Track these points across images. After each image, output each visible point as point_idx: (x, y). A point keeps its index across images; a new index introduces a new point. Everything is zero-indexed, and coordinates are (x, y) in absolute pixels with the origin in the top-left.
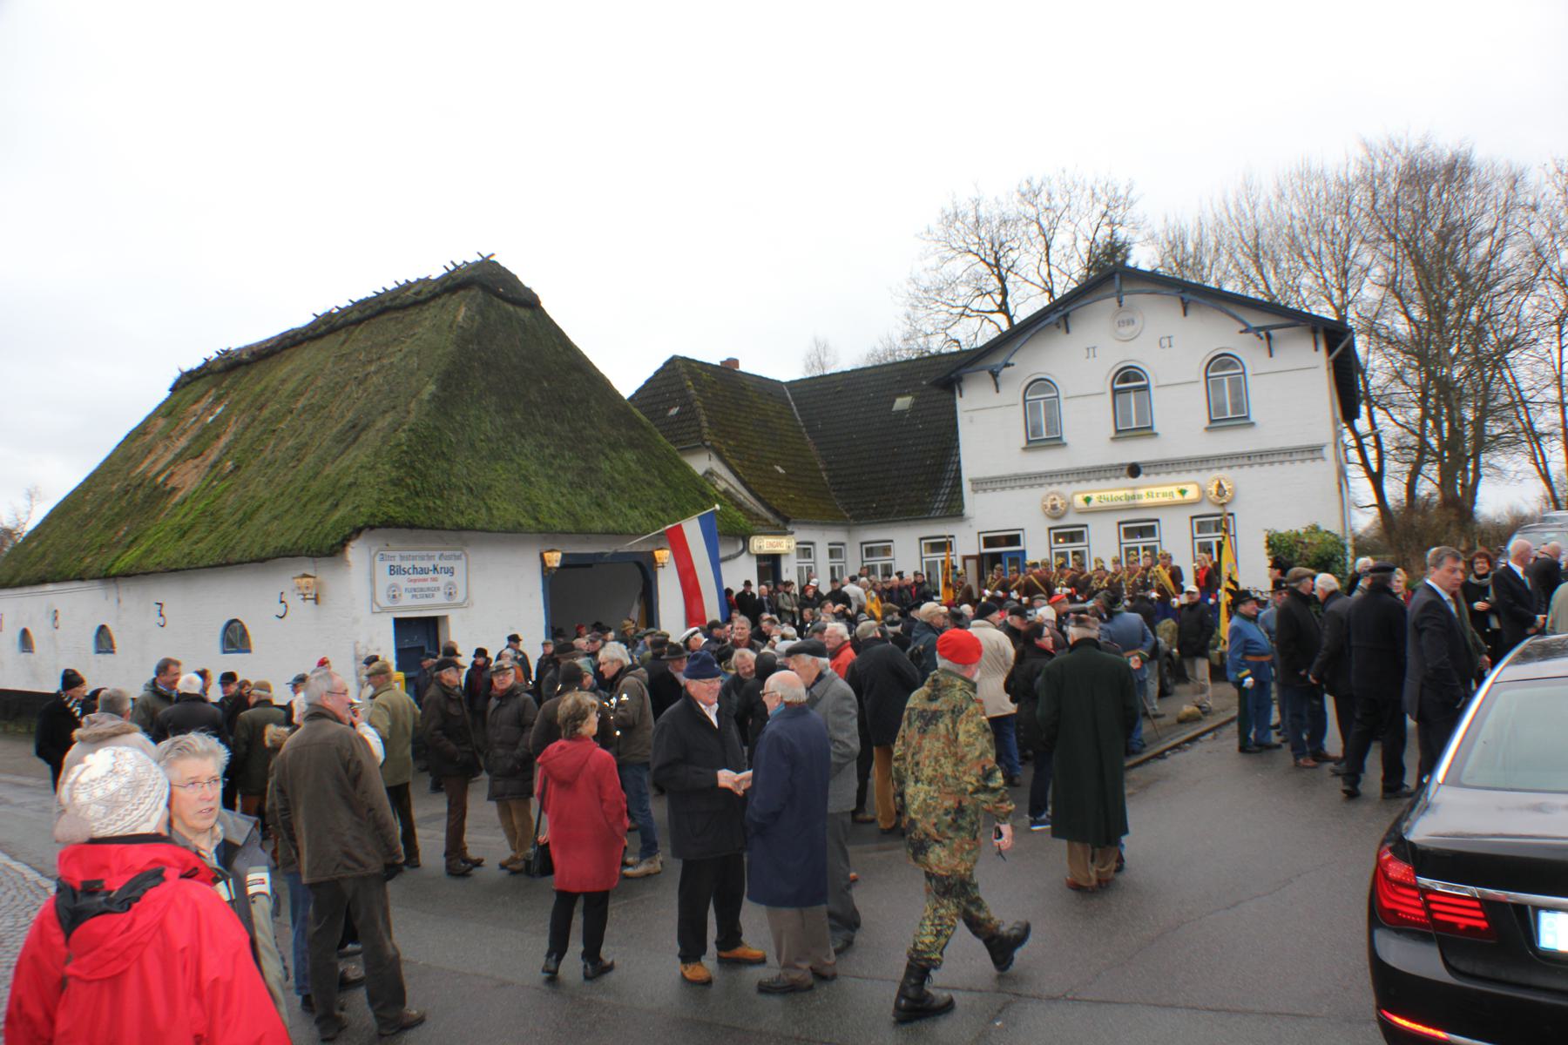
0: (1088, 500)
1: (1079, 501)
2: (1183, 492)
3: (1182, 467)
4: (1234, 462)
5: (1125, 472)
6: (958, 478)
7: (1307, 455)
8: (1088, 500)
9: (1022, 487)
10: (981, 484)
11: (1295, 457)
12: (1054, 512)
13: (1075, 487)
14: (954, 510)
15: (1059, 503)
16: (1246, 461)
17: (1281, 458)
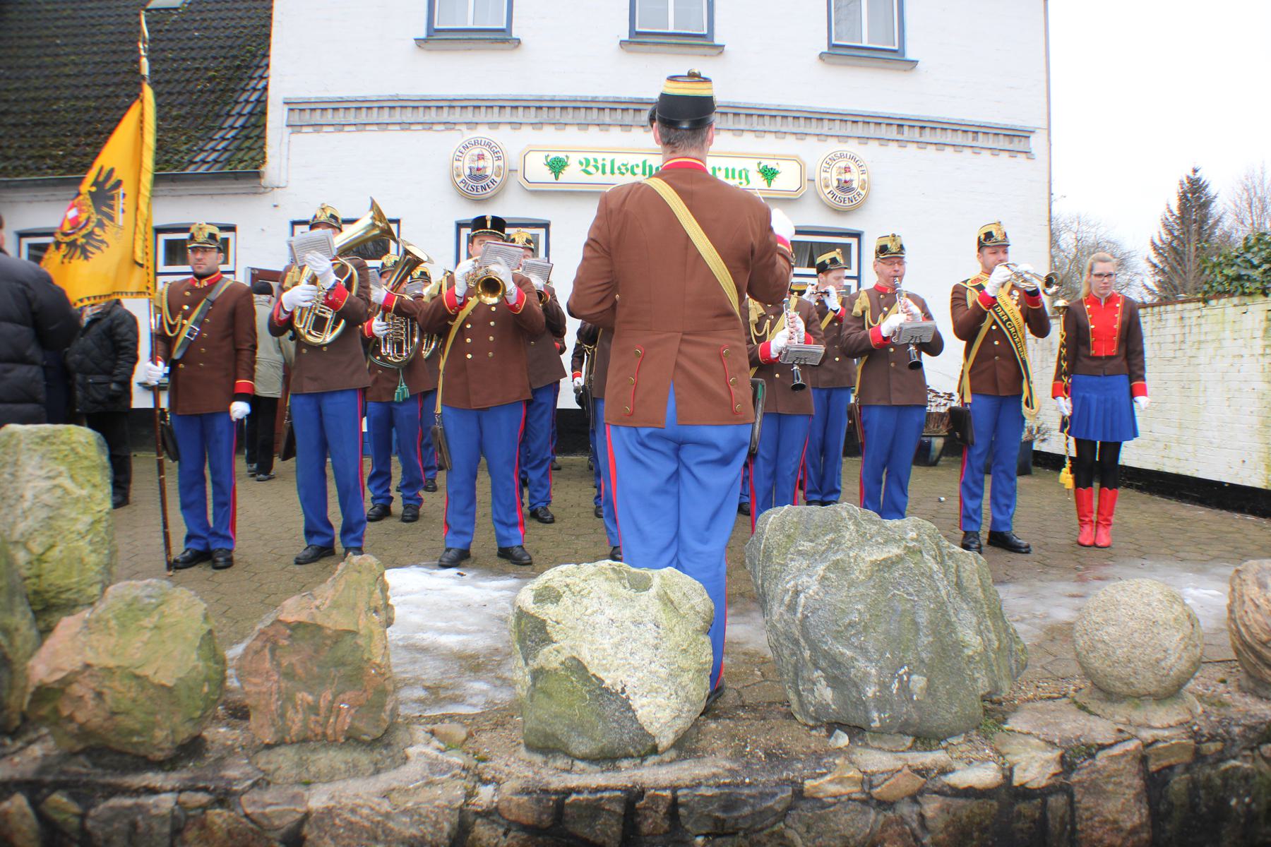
0: (557, 166)
1: (538, 170)
2: (769, 174)
3: (768, 124)
4: (872, 131)
5: (645, 116)
6: (262, 104)
7: (1003, 143)
8: (557, 166)
9: (405, 126)
10: (309, 114)
11: (982, 141)
12: (476, 184)
13: (528, 136)
14: (243, 167)
15: (489, 165)
16: (893, 133)
17: (959, 139)
